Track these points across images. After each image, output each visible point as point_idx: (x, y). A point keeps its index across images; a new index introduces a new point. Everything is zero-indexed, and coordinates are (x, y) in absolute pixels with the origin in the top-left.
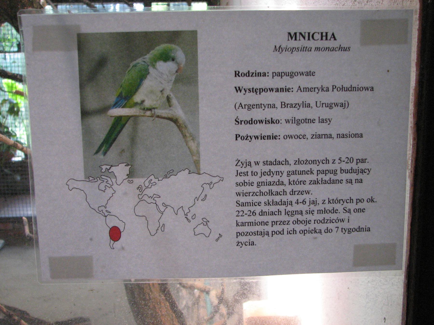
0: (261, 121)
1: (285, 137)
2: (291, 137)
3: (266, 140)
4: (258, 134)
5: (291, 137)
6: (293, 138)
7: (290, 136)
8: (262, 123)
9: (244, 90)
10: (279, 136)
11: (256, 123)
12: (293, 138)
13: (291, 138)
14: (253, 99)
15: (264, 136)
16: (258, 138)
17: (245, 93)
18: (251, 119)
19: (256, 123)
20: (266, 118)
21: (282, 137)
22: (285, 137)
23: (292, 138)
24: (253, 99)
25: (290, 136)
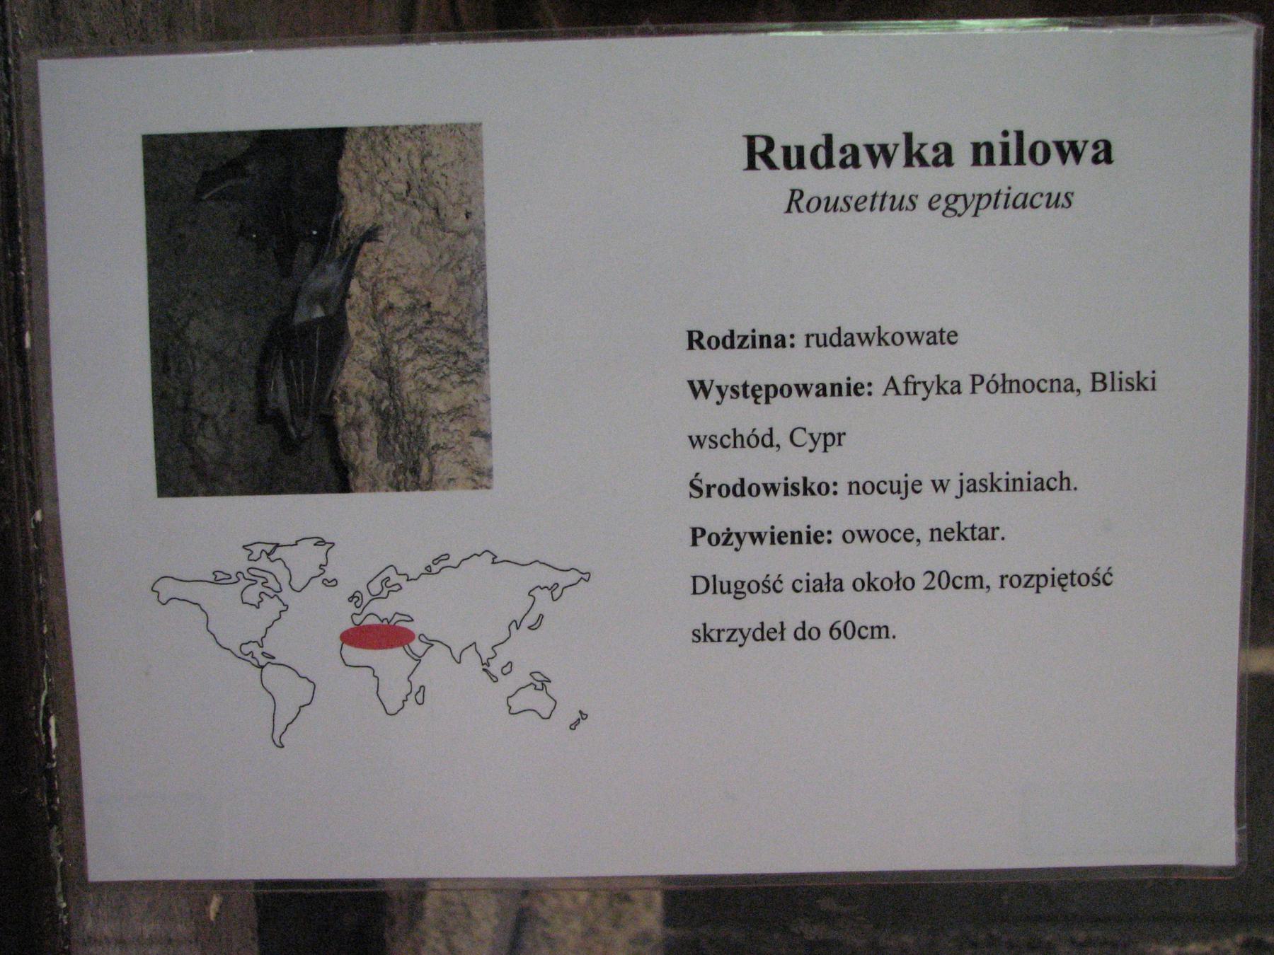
1: (849, 537)
2: (866, 536)
3: (788, 546)
5: (866, 536)
6: (874, 538)
7: (863, 533)
8: (776, 492)
9: (718, 392)
10: (829, 532)
12: (874, 538)
13: (866, 539)
14: (746, 416)
15: (780, 534)
17: (719, 399)
18: (739, 482)
21: (836, 537)
22: (849, 537)
23: (870, 540)
24: (746, 416)
25: (863, 533)
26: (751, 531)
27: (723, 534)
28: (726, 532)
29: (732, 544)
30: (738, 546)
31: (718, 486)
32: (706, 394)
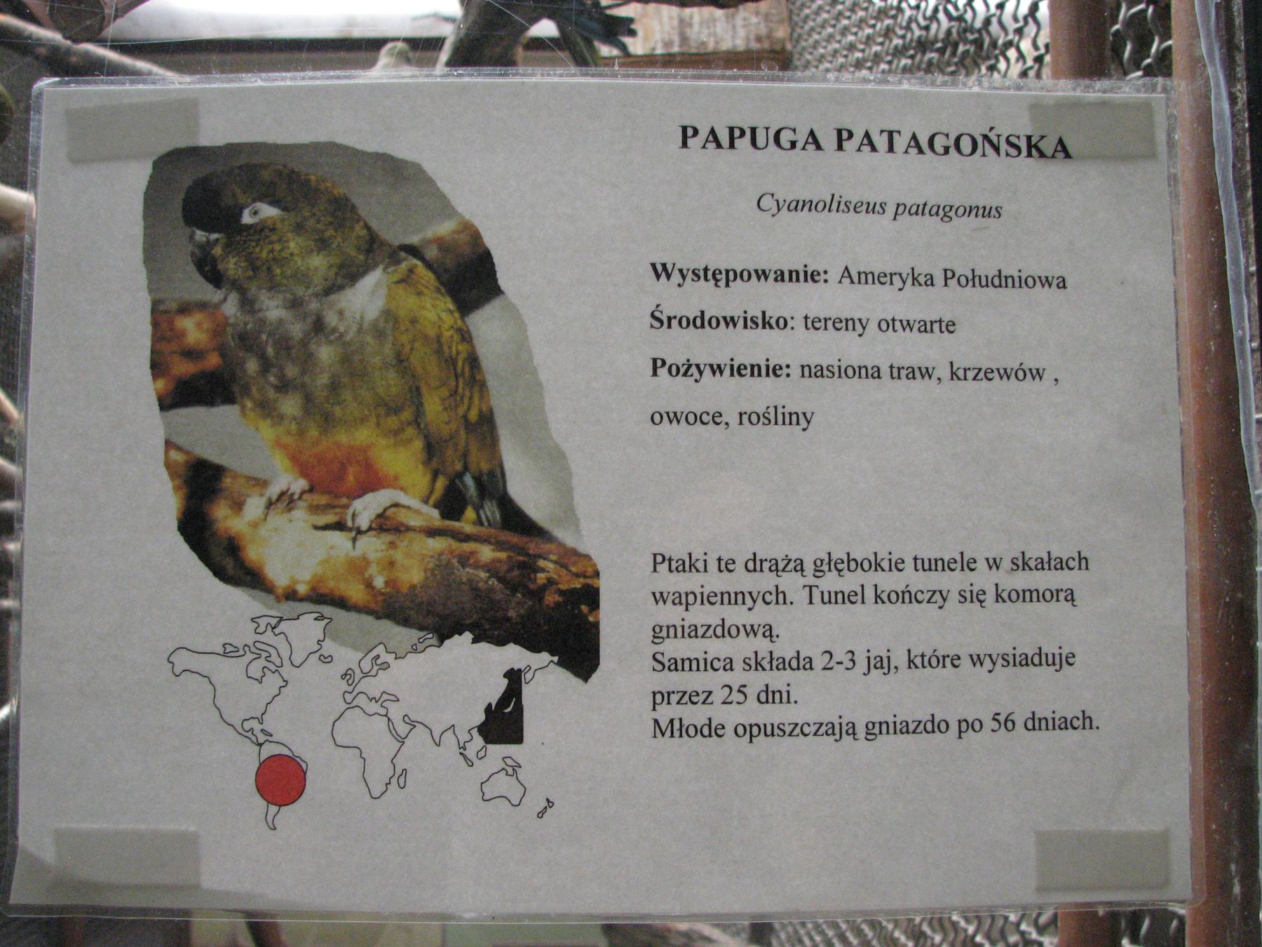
0: (732, 318)
4: (722, 358)
11: (714, 324)
16: (721, 373)
19: (714, 324)
20: (745, 312)
26: (711, 363)
27: (683, 365)
28: (686, 362)
29: (692, 375)
30: (698, 377)
31: (678, 318)
32: (669, 276)
